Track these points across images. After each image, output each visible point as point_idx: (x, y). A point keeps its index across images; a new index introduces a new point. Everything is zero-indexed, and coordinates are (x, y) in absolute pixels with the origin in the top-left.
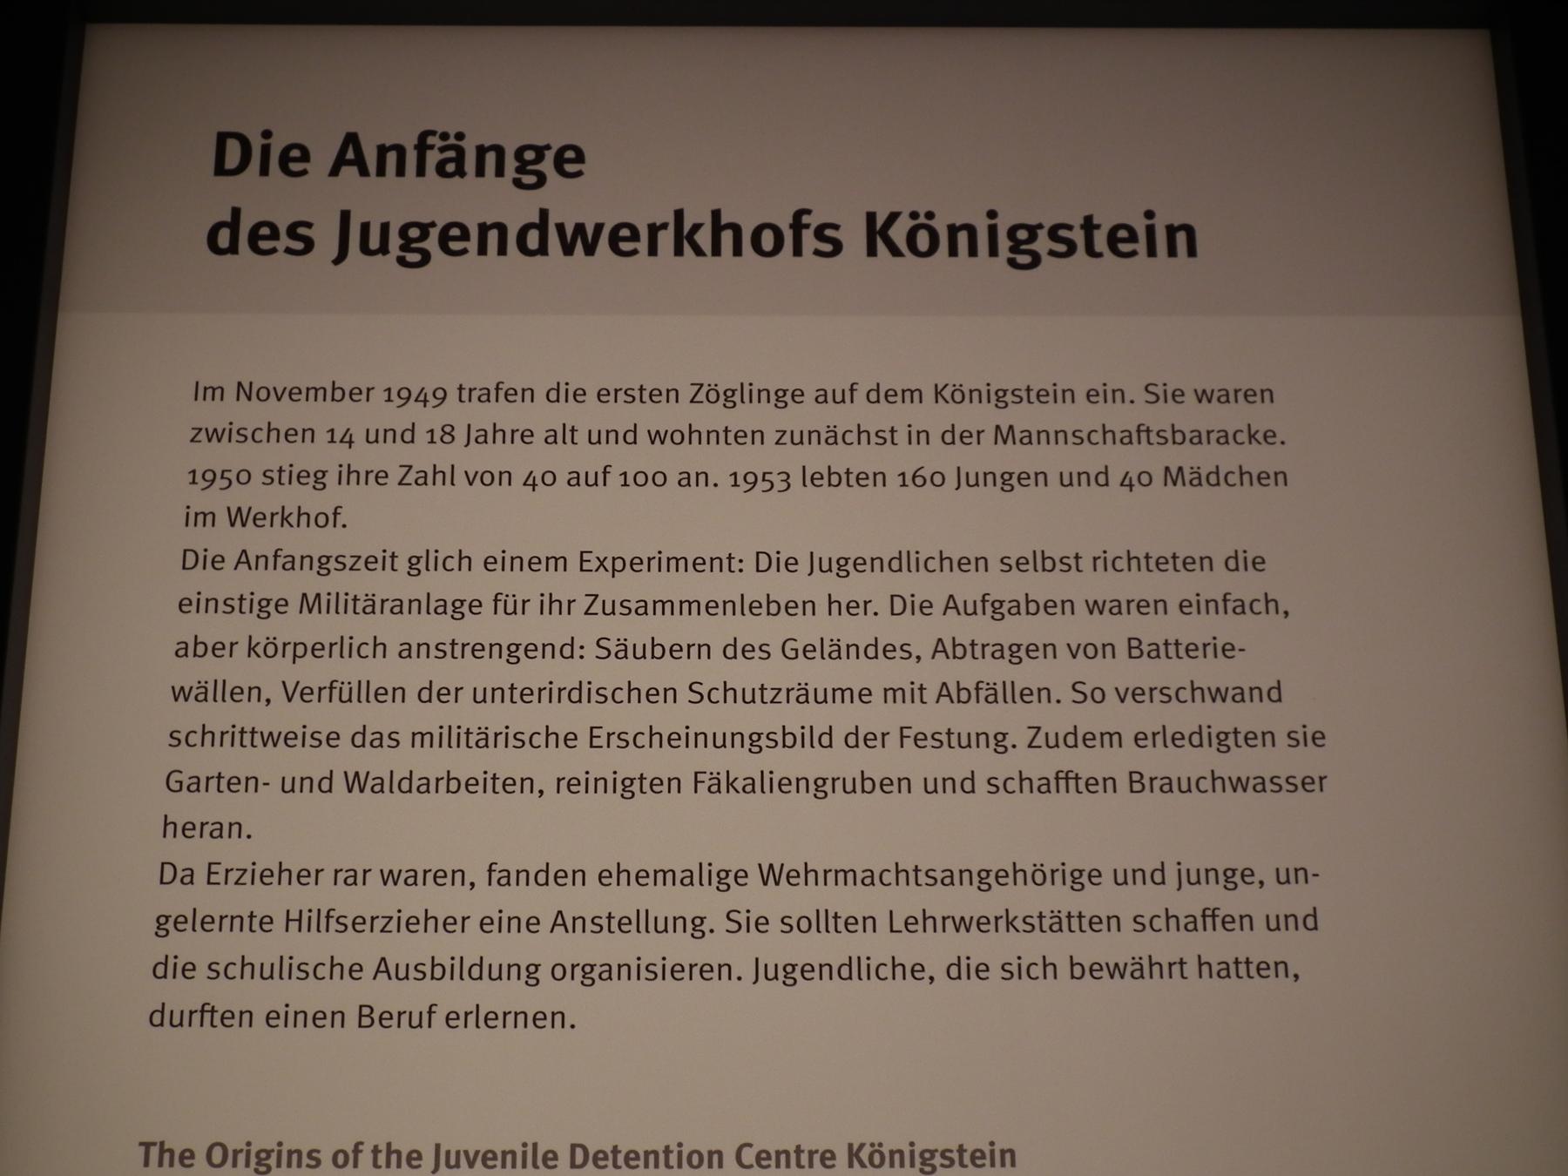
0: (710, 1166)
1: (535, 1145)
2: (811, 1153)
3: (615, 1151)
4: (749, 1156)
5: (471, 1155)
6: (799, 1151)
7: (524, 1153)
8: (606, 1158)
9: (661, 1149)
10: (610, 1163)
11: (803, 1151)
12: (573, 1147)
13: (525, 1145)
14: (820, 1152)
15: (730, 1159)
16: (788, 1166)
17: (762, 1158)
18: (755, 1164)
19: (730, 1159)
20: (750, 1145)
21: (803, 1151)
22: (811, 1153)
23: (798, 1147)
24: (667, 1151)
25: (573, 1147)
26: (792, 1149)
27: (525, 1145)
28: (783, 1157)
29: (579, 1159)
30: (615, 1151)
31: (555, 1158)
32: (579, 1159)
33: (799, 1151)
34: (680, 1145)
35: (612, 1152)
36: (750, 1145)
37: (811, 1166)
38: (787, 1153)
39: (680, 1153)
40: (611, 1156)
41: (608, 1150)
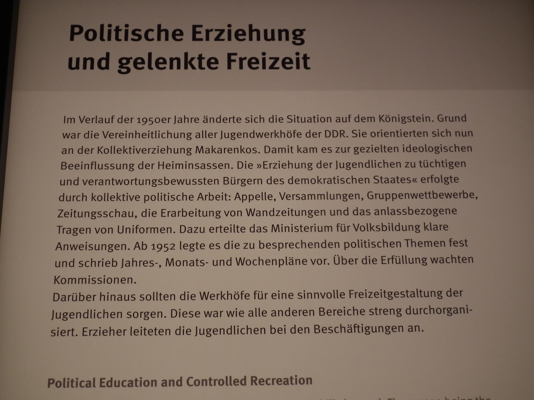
2: (215, 381)
4: (191, 382)
6: (210, 379)
11: (212, 380)
14: (218, 380)
16: (206, 385)
18: (194, 385)
20: (192, 378)
21: (212, 380)
22: (215, 381)
23: (210, 378)
26: (208, 379)
28: (204, 382)
33: (210, 379)
36: (192, 378)
37: (215, 385)
38: (206, 380)
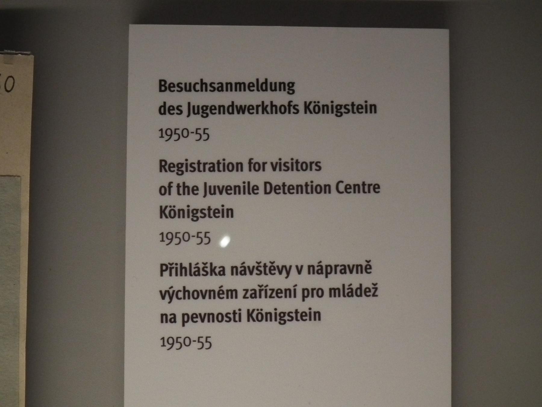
0: (325, 192)
1: (249, 183)
3: (284, 185)
5: (221, 188)
7: (244, 187)
8: (280, 189)
9: (303, 184)
10: (281, 191)
12: (266, 183)
13: (244, 183)
15: (333, 188)
17: (347, 188)
19: (333, 188)
20: (342, 182)
24: (307, 185)
25: (266, 183)
27: (244, 183)
29: (268, 190)
30: (284, 185)
31: (258, 189)
32: (268, 190)
34: (312, 182)
35: (282, 186)
39: (312, 186)
40: (282, 188)
41: (281, 184)
